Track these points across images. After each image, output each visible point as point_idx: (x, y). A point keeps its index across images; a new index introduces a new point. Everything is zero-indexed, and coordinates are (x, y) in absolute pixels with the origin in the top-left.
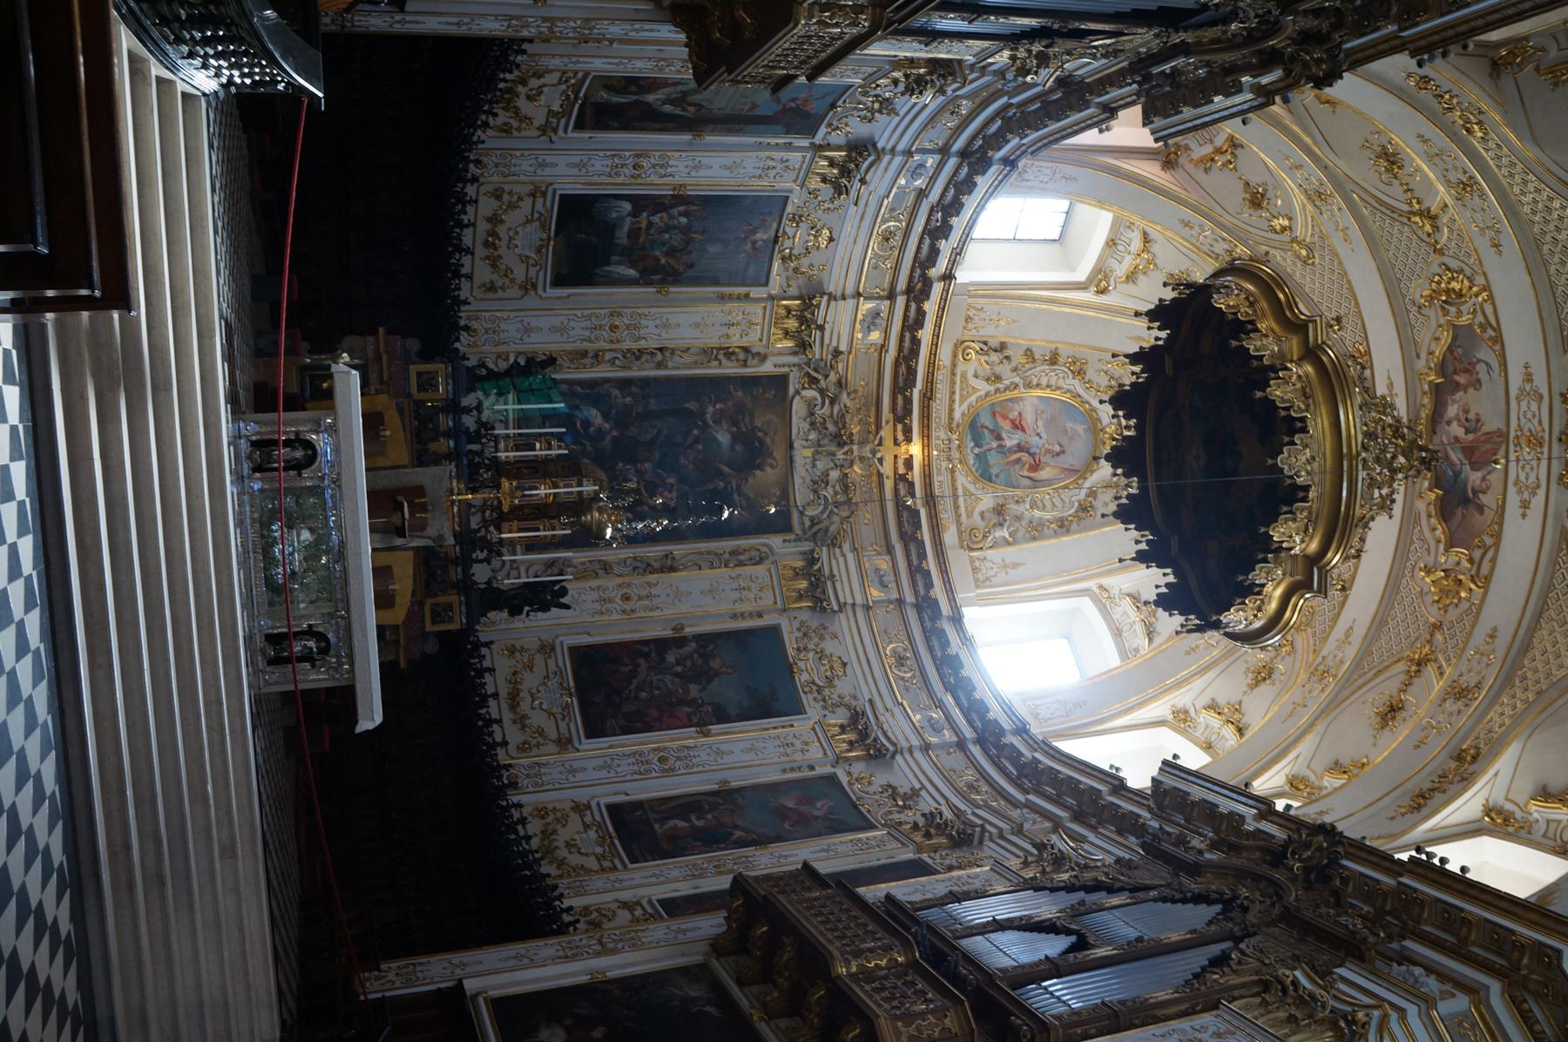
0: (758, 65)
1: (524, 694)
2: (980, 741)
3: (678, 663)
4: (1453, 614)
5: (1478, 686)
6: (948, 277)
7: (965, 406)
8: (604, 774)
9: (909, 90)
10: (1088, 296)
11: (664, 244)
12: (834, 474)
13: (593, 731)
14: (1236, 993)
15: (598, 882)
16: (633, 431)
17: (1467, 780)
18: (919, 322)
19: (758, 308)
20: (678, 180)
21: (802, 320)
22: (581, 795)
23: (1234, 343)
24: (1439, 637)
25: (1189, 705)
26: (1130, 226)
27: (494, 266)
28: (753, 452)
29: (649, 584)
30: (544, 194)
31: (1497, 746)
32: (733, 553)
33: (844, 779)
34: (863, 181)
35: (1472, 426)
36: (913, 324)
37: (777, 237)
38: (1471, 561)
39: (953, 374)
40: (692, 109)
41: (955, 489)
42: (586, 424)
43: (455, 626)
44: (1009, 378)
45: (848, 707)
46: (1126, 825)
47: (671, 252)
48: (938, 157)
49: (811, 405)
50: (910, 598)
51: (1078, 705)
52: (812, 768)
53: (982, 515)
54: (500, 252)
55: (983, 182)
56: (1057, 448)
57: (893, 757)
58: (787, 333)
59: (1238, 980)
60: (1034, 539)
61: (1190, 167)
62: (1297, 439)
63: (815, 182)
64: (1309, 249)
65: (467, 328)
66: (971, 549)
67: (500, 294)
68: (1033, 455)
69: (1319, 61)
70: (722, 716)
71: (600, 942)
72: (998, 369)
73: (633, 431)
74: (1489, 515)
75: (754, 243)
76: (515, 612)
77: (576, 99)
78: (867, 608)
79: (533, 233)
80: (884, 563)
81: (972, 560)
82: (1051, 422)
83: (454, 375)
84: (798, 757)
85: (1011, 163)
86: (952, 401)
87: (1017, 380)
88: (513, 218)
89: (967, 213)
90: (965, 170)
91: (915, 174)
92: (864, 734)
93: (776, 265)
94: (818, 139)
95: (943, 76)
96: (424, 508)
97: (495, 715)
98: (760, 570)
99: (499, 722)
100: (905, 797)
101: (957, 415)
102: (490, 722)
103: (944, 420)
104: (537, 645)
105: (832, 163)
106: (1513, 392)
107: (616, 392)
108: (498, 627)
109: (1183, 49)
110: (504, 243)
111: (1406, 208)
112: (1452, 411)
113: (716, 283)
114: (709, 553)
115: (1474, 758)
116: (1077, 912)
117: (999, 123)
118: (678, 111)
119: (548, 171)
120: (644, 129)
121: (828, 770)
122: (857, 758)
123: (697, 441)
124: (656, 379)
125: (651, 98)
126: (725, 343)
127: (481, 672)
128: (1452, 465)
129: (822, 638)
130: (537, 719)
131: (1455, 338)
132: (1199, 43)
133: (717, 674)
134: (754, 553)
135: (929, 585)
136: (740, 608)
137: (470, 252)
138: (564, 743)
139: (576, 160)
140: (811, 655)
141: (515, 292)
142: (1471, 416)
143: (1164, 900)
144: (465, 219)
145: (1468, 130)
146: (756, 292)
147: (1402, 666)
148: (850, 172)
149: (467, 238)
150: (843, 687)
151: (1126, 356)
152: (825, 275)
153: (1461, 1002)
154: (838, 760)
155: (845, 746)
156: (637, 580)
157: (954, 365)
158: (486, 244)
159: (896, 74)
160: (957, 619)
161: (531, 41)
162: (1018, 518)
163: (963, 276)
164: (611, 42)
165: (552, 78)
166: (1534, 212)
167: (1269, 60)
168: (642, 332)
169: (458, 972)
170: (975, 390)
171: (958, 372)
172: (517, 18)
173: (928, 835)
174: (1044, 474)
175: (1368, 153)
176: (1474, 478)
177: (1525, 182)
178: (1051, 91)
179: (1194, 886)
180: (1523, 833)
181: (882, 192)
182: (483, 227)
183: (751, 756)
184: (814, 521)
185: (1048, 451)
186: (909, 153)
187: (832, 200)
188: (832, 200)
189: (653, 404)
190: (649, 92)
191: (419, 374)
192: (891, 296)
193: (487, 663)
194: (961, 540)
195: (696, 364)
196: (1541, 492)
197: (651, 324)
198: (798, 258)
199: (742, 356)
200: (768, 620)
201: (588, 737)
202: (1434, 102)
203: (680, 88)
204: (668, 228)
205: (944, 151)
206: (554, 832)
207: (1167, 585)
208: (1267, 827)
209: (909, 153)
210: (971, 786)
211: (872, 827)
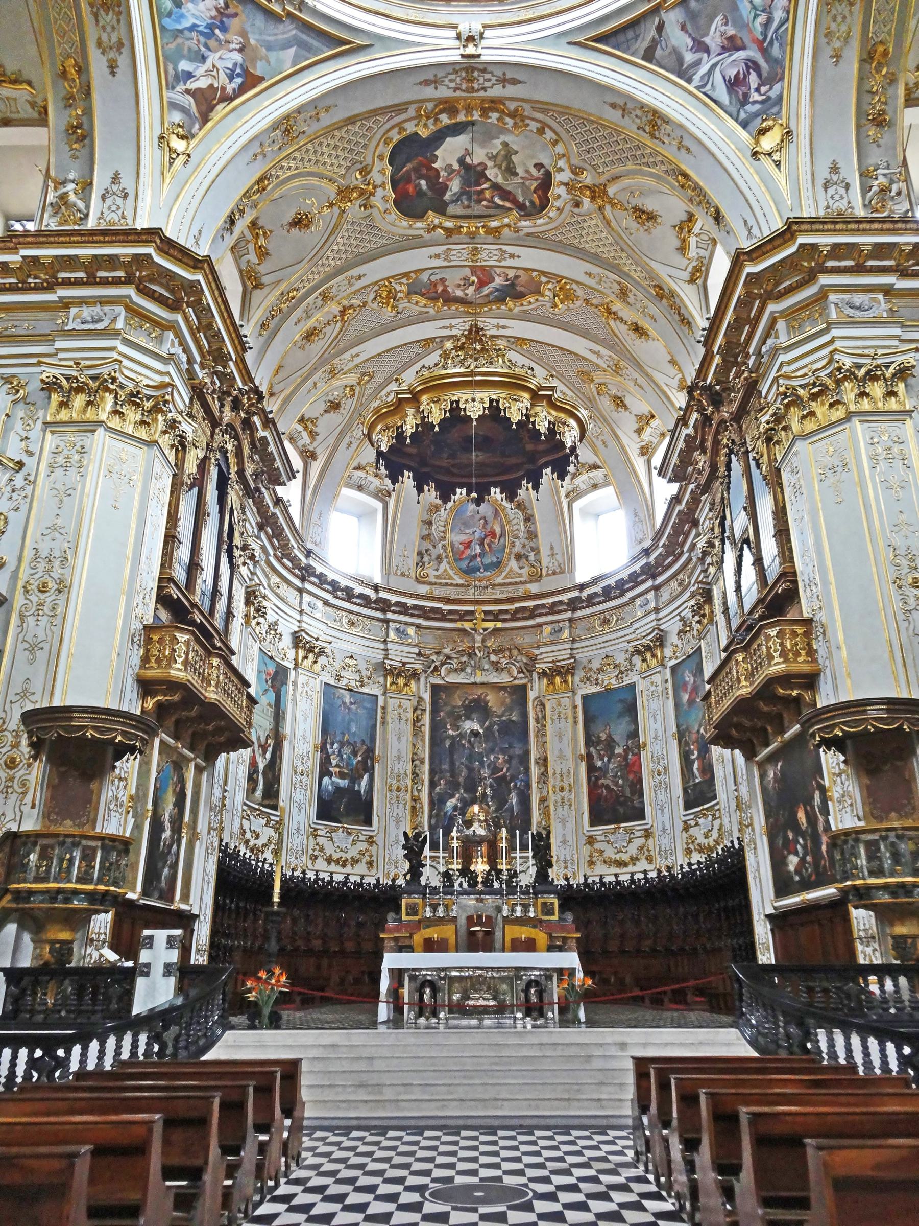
0: (238, 716)
1: (618, 857)
2: (654, 577)
3: (602, 759)
4: (580, 292)
5: (619, 283)
6: (376, 588)
7: (455, 577)
8: (666, 810)
9: (264, 615)
10: (392, 502)
11: (349, 758)
12: (493, 658)
13: (641, 815)
14: (772, 457)
15: (726, 821)
16: (461, 780)
17: (673, 294)
18: (404, 605)
19: (391, 701)
20: (311, 749)
21: (399, 675)
22: (680, 826)
23: (408, 441)
24: (595, 301)
25: (638, 446)
26: (350, 477)
27: (357, 861)
28: (478, 708)
29: (554, 774)
30: (316, 830)
31: (651, 275)
32: (537, 721)
33: (674, 662)
34: (317, 639)
35: (467, 283)
36: (404, 609)
37: (349, 690)
38: (548, 282)
39: (436, 584)
41: (505, 584)
42: (455, 808)
43: (556, 901)
44: (439, 550)
45: (632, 656)
46: (695, 501)
47: (355, 754)
48: (305, 595)
49: (450, 671)
50: (569, 615)
51: (636, 515)
52: (667, 681)
53: (521, 568)
54: (349, 857)
55: (319, 569)
56: (482, 521)
57: (662, 631)
58: (406, 685)
59: (766, 456)
60: (536, 536)
61: (315, 444)
62: (462, 406)
63: (317, 667)
64: (364, 374)
65: (394, 880)
66: (541, 576)
67: (374, 858)
68: (486, 536)
69: (249, 399)
70: (634, 734)
71: (747, 827)
72: (434, 557)
73: (461, 780)
74: (520, 272)
75: (351, 703)
76: (551, 865)
78: (573, 641)
79: (339, 836)
80: (547, 630)
81: (548, 575)
82: (466, 524)
83: (410, 893)
84: (659, 688)
85: (309, 553)
86: (452, 585)
87: (440, 545)
88: (329, 849)
89: (337, 578)
90: (313, 579)
92: (648, 648)
93: (365, 690)
94: (291, 665)
95: (256, 597)
96: (480, 917)
97: (628, 877)
98: (548, 706)
99: (632, 874)
100: (685, 625)
101: (460, 581)
102: (632, 881)
103: (462, 589)
104: (588, 847)
105: (306, 658)
106: (446, 264)
107: (437, 789)
108: (556, 875)
109: (241, 473)
110: (342, 854)
111: (339, 324)
112: (459, 293)
113: (375, 726)
114: (537, 736)
115: (661, 288)
116: (733, 543)
117: (285, 561)
118: (270, 750)
119: (302, 827)
120: (280, 770)
121: (668, 671)
122: (662, 652)
123: (469, 741)
124: (431, 764)
125: (261, 766)
126: (410, 723)
127: (603, 884)
128: (491, 293)
129: (591, 669)
130: (633, 850)
131: (416, 293)
132: (238, 464)
133: (609, 736)
134: (538, 709)
135: (561, 602)
136: (570, 719)
137: (347, 878)
138: (648, 834)
139: (296, 810)
140: (600, 677)
141: (374, 849)
142: (462, 283)
143: (729, 488)
144: (327, 878)
146: (381, 703)
147: (612, 323)
149: (339, 878)
150: (620, 658)
152: (373, 661)
153: (781, 325)
154: (663, 665)
155: (654, 660)
156: (551, 781)
157: (430, 583)
158: (344, 866)
159: (254, 623)
160: (582, 587)
161: (221, 841)
162: (524, 546)
163: (378, 580)
164: (226, 791)
165: (246, 824)
166: (340, 258)
167: (247, 424)
168: (402, 772)
169: (762, 917)
170: (445, 571)
171: (434, 580)
172: (207, 849)
173: (704, 616)
174: (498, 530)
175: (307, 346)
176: (499, 281)
177: (323, 265)
178: (266, 533)
179: (722, 469)
180: (705, 262)
181: (324, 627)
182: (333, 867)
183: (658, 717)
184: (519, 672)
185: (484, 527)
186: (301, 612)
187: (328, 657)
188: (328, 657)
189: (446, 766)
191: (408, 914)
192: (387, 621)
193: (597, 879)
194: (536, 581)
195: (423, 740)
196: (504, 248)
197: (398, 766)
198: (362, 677)
199: (419, 712)
200: (579, 702)
201: (644, 819)
202: (276, 319)
204: (340, 755)
206: (699, 845)
207: (553, 473)
208: (692, 422)
209: (301, 612)
210: (680, 584)
211: (700, 647)
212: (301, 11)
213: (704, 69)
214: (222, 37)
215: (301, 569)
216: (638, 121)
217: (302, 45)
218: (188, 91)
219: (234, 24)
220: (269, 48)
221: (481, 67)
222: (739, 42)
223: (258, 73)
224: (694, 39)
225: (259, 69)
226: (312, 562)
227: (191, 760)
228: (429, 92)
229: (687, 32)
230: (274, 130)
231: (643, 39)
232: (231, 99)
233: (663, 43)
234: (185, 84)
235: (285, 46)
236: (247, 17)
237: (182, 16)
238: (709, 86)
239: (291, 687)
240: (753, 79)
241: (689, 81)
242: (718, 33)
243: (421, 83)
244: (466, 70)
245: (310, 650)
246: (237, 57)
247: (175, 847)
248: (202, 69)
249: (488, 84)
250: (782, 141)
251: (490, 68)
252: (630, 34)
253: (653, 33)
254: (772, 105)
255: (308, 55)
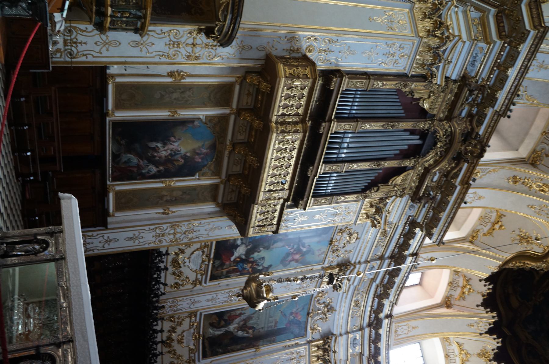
34: (335, 352)
40: (250, 331)
55: (383, 331)
61: (457, 303)
77: (199, 337)
90: (373, 332)
91: (354, 344)
94: (309, 338)
105: (319, 348)
145: (543, 191)
148: (327, 349)
151: (486, 333)
165: (186, 324)
190: (230, 324)
203: (243, 317)
205: (361, 329)
215: (377, 318)
226: (386, 322)
227: (220, 178)
239: (294, 343)
245: (326, 351)
247: (154, 170)
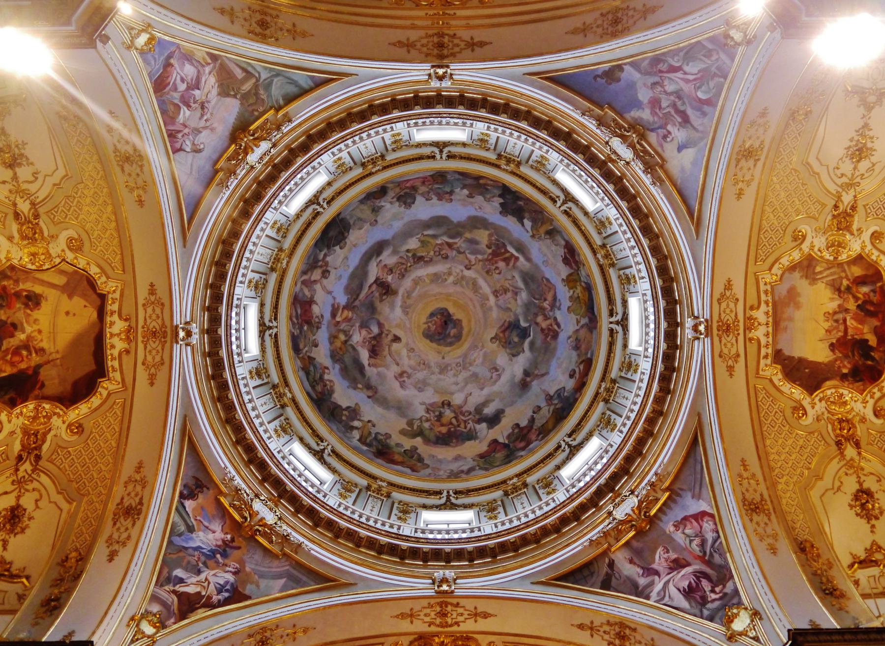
212: (296, 553)
213: (659, 587)
214: (221, 560)
216: (606, 637)
217: (290, 577)
218: (174, 592)
219: (236, 553)
220: (262, 576)
221: (455, 601)
222: (684, 562)
223: (247, 592)
224: (642, 568)
225: (249, 589)
228: (405, 626)
229: (635, 564)
230: (250, 636)
231: (598, 575)
232: (214, 607)
233: (617, 575)
234: (174, 586)
235: (279, 576)
236: (248, 551)
237: (192, 539)
238: (667, 598)
240: (706, 585)
241: (648, 598)
242: (663, 560)
243: (397, 617)
244: (441, 604)
246: (231, 578)
248: (194, 579)
249: (460, 619)
250: (752, 621)
251: (462, 602)
252: (586, 572)
253: (605, 569)
254: (732, 600)
255: (294, 585)
